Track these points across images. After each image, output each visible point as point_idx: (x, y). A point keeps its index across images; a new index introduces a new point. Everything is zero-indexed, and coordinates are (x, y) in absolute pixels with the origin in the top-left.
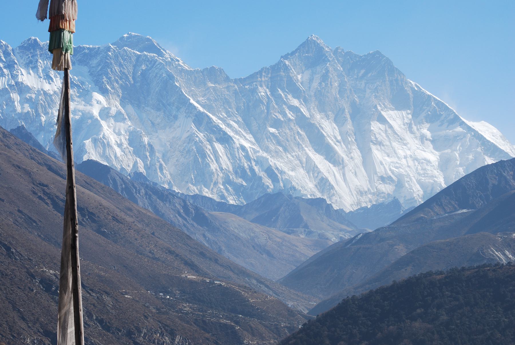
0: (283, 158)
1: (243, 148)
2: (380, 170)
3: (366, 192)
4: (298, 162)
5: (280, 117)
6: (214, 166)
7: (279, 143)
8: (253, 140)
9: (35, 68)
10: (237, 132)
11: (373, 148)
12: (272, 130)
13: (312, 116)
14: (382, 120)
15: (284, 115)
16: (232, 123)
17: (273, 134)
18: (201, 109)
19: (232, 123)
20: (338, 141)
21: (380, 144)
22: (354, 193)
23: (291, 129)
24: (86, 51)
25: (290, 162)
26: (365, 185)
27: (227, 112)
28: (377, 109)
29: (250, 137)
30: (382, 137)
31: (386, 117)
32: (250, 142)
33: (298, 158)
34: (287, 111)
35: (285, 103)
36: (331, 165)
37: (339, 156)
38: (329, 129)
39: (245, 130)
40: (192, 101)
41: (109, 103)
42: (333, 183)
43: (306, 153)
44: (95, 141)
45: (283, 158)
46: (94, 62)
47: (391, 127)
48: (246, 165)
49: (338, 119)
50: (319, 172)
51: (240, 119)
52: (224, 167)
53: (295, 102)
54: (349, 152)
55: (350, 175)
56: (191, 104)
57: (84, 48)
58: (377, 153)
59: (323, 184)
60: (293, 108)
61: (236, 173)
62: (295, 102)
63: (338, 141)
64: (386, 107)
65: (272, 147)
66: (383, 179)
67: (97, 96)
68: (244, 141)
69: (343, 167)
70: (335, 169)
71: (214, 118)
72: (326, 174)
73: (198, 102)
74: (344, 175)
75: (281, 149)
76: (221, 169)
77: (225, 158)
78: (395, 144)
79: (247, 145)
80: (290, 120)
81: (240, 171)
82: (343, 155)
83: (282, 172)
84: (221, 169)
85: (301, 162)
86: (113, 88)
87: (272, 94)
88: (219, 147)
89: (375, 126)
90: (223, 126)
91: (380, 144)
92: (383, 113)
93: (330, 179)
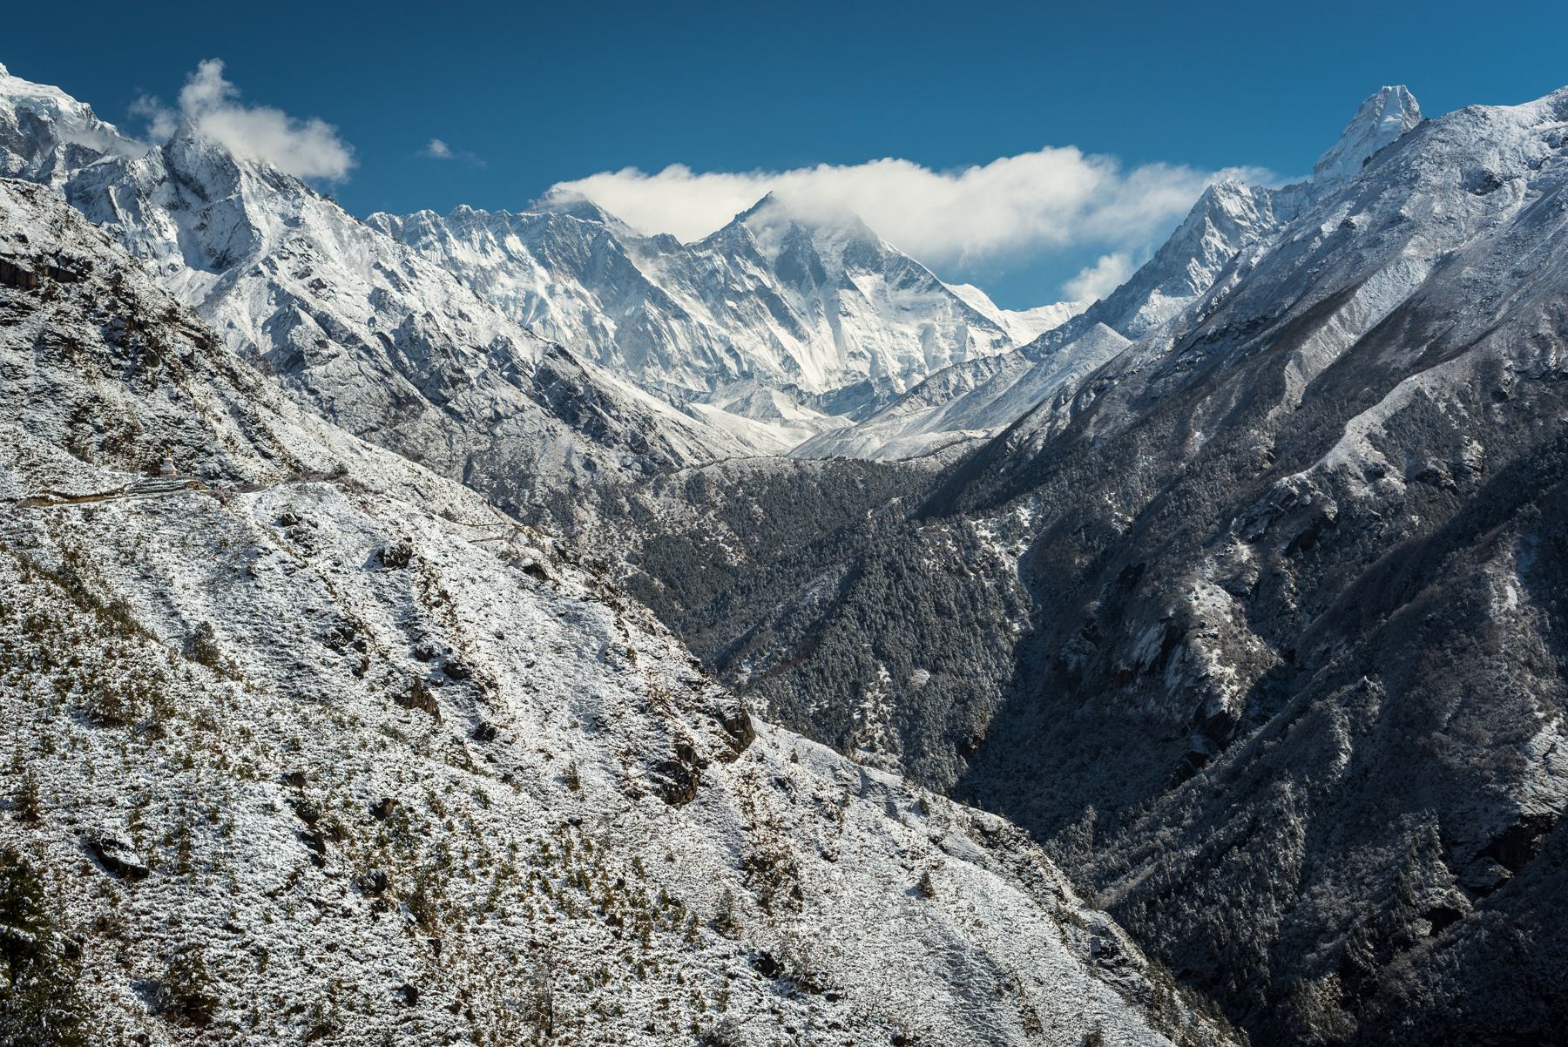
5: (739, 288)
7: (739, 318)
12: (730, 303)
14: (853, 287)
15: (743, 284)
21: (848, 314)
34: (747, 281)
44: (544, 322)
46: (534, 231)
59: (789, 363)
60: (751, 277)
62: (756, 271)
67: (540, 271)
70: (800, 345)
79: (706, 323)
91: (848, 314)
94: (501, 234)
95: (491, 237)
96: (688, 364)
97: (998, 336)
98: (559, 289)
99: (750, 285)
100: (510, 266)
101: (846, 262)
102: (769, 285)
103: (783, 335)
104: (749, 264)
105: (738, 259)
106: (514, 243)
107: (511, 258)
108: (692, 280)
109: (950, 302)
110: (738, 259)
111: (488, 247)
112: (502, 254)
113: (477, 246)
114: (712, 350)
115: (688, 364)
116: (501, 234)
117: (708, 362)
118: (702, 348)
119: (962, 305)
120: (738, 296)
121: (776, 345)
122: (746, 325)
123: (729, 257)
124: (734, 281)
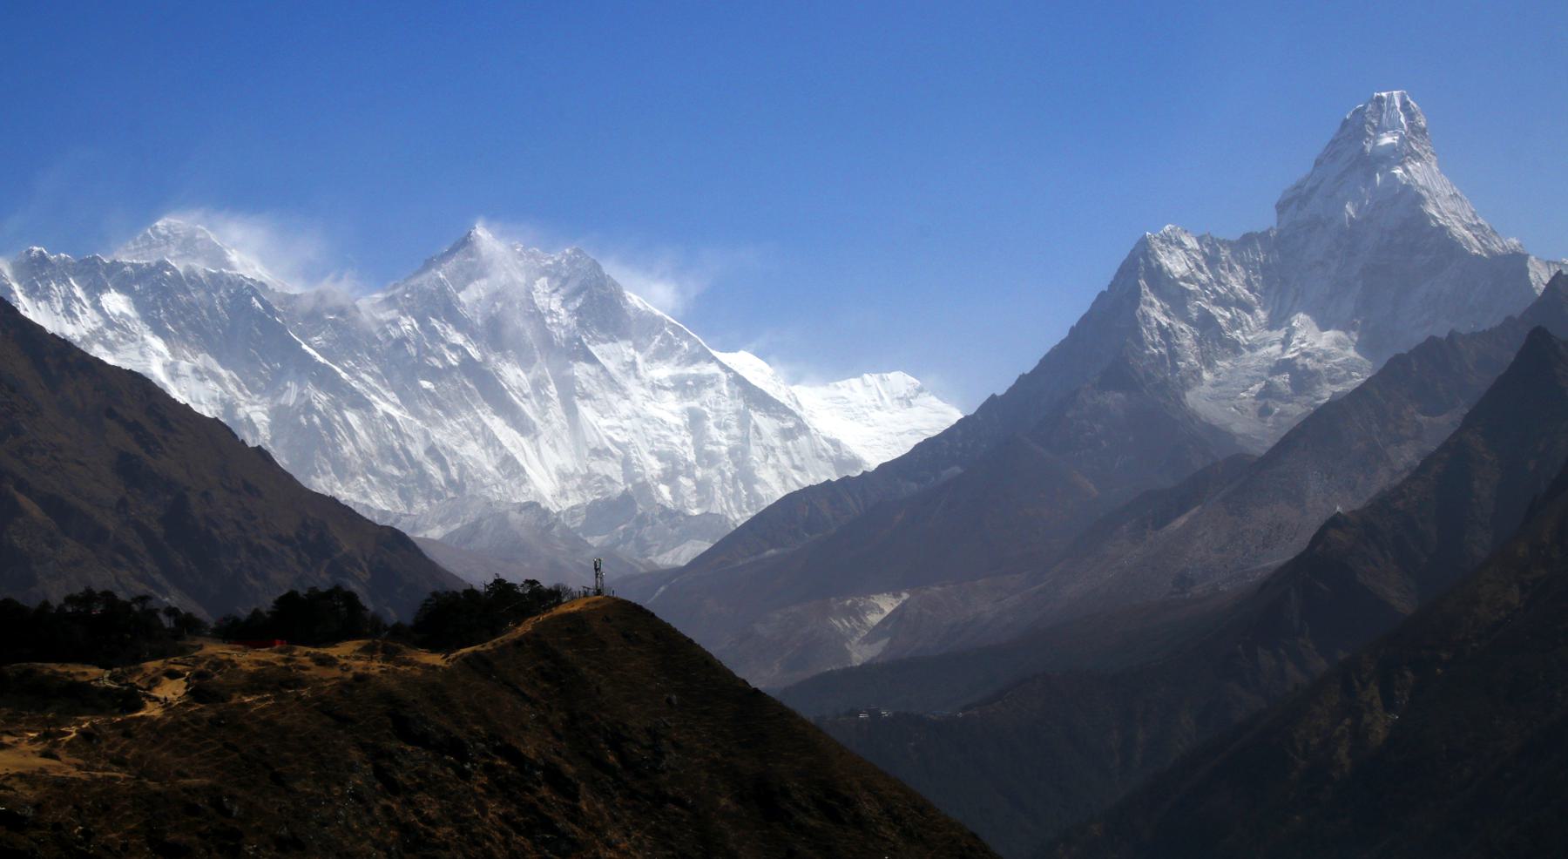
0: (444, 428)
1: (390, 418)
2: (593, 440)
3: (572, 475)
4: (466, 432)
5: (438, 363)
6: (347, 449)
7: (438, 404)
8: (398, 401)
9: (47, 298)
10: (374, 391)
11: (578, 403)
12: (426, 384)
13: (486, 360)
14: (590, 359)
15: (443, 358)
16: (364, 376)
17: (427, 391)
18: (321, 359)
19: (364, 376)
20: (525, 396)
22: (555, 477)
23: (454, 382)
24: (128, 269)
25: (455, 432)
26: (568, 462)
27: (354, 358)
28: (581, 343)
29: (392, 396)
30: (590, 386)
31: (596, 355)
32: (398, 408)
33: (467, 425)
34: (447, 353)
35: (443, 341)
36: (514, 433)
37: (528, 419)
38: (512, 375)
39: (384, 386)
40: (305, 347)
41: (173, 354)
42: (522, 462)
43: (480, 419)
45: (444, 428)
47: (604, 369)
48: (396, 444)
49: (526, 362)
50: (501, 447)
51: (376, 369)
52: (363, 447)
53: (458, 339)
54: (544, 412)
55: (546, 449)
56: (304, 351)
57: (123, 265)
58: (586, 411)
60: (454, 348)
61: (382, 455)
62: (458, 339)
63: (525, 396)
64: (595, 338)
65: (428, 411)
66: (600, 453)
68: (386, 405)
69: (536, 437)
70: (523, 441)
71: (338, 370)
72: (512, 450)
73: (310, 345)
74: (538, 450)
75: (440, 413)
76: (360, 452)
77: (363, 433)
78: (613, 397)
79: (396, 413)
80: (451, 366)
81: (389, 454)
82: (534, 418)
83: (453, 454)
84: (360, 452)
85: (472, 431)
86: (178, 329)
87: (421, 327)
88: (352, 417)
89: (580, 370)
90: (355, 384)
92: (592, 349)
93: (517, 456)
94: (95, 289)
95: (79, 292)
96: (375, 472)
97: (790, 424)
98: (184, 366)
99: (453, 359)
100: (110, 334)
101: (580, 324)
102: (476, 354)
103: (497, 425)
104: (450, 330)
105: (435, 323)
106: (115, 302)
107: (110, 324)
108: (371, 353)
109: (723, 376)
110: (435, 323)
111: (76, 308)
112: (97, 318)
113: (59, 307)
114: (407, 453)
115: (375, 472)
116: (95, 289)
117: (401, 467)
118: (392, 448)
119: (739, 380)
120: (434, 374)
121: (491, 441)
122: (449, 414)
123: (422, 321)
124: (430, 353)
